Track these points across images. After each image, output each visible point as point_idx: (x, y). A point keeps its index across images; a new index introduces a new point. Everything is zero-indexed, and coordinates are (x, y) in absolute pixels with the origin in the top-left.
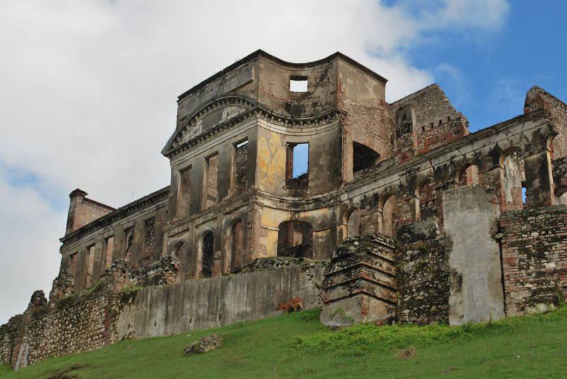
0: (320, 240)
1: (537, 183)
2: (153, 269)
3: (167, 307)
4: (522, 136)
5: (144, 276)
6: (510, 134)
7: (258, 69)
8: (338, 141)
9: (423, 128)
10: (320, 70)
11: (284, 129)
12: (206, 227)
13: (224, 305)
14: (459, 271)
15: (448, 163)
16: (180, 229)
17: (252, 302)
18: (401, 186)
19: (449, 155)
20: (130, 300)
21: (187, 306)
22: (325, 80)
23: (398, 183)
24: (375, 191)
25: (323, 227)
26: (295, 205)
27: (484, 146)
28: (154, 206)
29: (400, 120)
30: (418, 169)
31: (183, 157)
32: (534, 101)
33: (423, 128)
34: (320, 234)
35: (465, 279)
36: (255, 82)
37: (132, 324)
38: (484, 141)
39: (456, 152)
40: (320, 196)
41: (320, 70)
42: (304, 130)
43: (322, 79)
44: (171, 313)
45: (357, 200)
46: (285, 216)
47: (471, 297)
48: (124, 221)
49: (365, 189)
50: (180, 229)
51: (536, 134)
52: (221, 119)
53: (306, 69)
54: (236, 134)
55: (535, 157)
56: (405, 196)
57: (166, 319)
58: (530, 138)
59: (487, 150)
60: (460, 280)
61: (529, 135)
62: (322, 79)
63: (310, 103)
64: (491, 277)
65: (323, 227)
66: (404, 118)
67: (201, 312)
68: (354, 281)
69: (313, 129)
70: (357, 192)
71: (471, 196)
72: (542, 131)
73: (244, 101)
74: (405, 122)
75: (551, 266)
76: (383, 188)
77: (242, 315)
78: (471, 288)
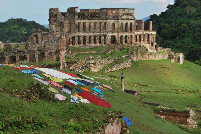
16: (122, 33)
50: (122, 33)
59: (151, 33)
61: (154, 33)
70: (136, 33)
77: (161, 58)
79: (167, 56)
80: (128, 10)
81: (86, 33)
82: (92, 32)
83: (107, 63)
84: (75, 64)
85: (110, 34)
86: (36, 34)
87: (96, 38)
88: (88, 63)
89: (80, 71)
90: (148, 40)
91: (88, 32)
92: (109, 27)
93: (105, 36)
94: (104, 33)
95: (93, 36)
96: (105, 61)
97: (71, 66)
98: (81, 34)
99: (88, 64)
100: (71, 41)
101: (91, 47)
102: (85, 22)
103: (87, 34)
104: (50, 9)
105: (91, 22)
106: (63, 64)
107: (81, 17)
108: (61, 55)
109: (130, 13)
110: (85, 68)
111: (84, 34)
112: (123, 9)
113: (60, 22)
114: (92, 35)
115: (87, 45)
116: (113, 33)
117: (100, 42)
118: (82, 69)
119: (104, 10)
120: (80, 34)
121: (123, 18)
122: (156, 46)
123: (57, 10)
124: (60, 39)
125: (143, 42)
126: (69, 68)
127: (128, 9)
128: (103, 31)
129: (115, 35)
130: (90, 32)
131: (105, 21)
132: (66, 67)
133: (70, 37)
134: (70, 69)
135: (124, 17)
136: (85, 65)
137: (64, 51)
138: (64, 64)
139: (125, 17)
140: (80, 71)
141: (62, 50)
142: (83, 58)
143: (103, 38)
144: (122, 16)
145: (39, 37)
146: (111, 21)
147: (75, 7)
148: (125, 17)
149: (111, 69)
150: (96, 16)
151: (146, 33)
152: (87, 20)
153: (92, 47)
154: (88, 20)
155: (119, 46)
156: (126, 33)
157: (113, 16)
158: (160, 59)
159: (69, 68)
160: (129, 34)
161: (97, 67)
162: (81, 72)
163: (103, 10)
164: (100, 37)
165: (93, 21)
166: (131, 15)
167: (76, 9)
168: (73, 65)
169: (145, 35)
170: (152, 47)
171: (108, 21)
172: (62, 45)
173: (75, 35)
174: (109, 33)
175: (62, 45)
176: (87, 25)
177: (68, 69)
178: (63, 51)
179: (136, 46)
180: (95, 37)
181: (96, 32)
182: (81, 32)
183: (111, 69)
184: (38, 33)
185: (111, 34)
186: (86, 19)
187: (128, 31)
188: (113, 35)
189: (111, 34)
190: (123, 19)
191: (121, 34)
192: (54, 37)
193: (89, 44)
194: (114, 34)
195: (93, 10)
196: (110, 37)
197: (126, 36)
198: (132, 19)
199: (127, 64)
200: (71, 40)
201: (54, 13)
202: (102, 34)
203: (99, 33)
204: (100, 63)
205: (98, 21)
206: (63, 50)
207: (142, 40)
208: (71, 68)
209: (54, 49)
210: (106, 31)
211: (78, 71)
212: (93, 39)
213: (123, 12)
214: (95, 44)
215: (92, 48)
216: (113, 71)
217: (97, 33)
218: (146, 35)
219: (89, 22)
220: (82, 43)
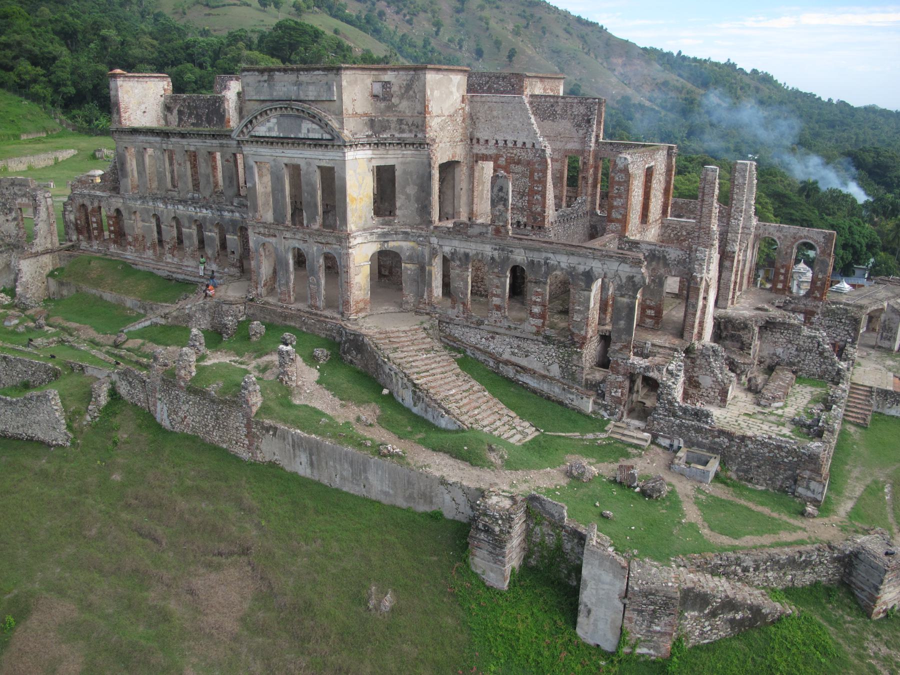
0: (409, 272)
1: (622, 323)
2: (229, 212)
4: (616, 274)
6: (605, 266)
7: (340, 87)
9: (506, 141)
10: (405, 77)
11: (370, 152)
13: (366, 478)
14: (590, 606)
15: (543, 262)
18: (492, 258)
19: (544, 255)
20: (271, 433)
22: (411, 93)
23: (490, 254)
24: (467, 251)
25: (411, 259)
26: (384, 235)
27: (579, 264)
30: (511, 252)
32: (621, 171)
33: (506, 141)
34: (409, 266)
35: (593, 612)
36: (337, 103)
37: (277, 453)
38: (580, 260)
39: (551, 255)
40: (409, 230)
41: (405, 77)
42: (390, 152)
43: (407, 91)
46: (375, 248)
47: (595, 625)
48: (184, 142)
49: (456, 243)
51: (631, 278)
52: (300, 132)
53: (389, 73)
54: (321, 157)
56: (496, 270)
58: (624, 280)
59: (581, 269)
60: (589, 612)
62: (407, 91)
63: (395, 119)
64: (613, 622)
65: (411, 259)
66: (501, 189)
67: (345, 473)
68: (497, 555)
69: (399, 152)
70: (447, 242)
71: (608, 563)
72: (636, 279)
74: (501, 194)
75: (658, 628)
76: (474, 252)
78: (596, 620)
98: (139, 202)
121: (261, 130)
135: (268, 125)
151: (537, 257)
217: (204, 211)
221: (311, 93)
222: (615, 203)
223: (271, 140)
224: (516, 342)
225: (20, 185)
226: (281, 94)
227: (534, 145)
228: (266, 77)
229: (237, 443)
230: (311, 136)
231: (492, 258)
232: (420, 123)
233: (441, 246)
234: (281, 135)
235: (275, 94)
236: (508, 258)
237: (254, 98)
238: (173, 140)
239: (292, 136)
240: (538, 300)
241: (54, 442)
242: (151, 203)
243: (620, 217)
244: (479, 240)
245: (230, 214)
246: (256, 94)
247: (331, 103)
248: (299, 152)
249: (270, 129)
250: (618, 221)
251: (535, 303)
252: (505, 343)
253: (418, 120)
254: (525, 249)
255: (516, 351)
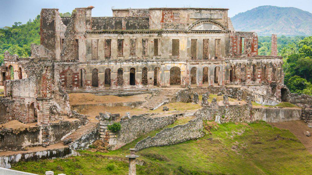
3: (267, 114)
5: (146, 63)
8: (228, 41)
12: (206, 65)
13: (279, 116)
15: (260, 62)
17: (285, 116)
19: (261, 60)
20: (257, 111)
21: (271, 114)
23: (247, 62)
24: (240, 62)
28: (148, 35)
29: (248, 43)
30: (252, 60)
31: (194, 35)
32: (256, 37)
37: (258, 117)
39: (262, 60)
44: (268, 116)
45: (235, 63)
49: (237, 61)
51: (280, 62)
52: (212, 28)
54: (217, 36)
55: (279, 69)
56: (248, 67)
57: (267, 117)
58: (279, 63)
59: (269, 62)
61: (279, 62)
67: (274, 116)
73: (219, 25)
76: (242, 62)
77: (283, 118)
79: (301, 114)
80: (209, 12)
81: (110, 62)
82: (126, 61)
83: (146, 129)
84: (74, 130)
85: (170, 65)
86: (9, 64)
87: (136, 73)
88: (101, 127)
89: (83, 145)
90: (264, 78)
91: (116, 62)
92: (167, 49)
93: (156, 70)
94: (155, 62)
95: (127, 70)
96: (141, 124)
97: (64, 134)
98: (99, 64)
99: (102, 130)
100: (77, 79)
101: (122, 94)
102: (108, 38)
103: (113, 64)
104: (44, 11)
105: (123, 38)
106: (45, 129)
107: (104, 28)
108: (41, 110)
109: (212, 18)
110: (96, 138)
111: (106, 64)
112: (197, 9)
113: (61, 39)
114: (125, 67)
115: (115, 88)
116: (175, 62)
117: (145, 82)
118: (88, 139)
119: (156, 11)
120: (98, 66)
121: (197, 28)
122: (283, 91)
123: (54, 12)
124: (39, 78)
125: (251, 82)
126: (58, 137)
127: (210, 10)
128: (152, 58)
129: (179, 66)
130: (121, 61)
131: (155, 36)
132: (53, 135)
133: (74, 70)
134: (62, 139)
135: (200, 27)
136: (95, 132)
137: (47, 103)
138: (46, 129)
139: (201, 27)
140: (83, 145)
141: (42, 100)
142: (95, 116)
143: (150, 74)
144: (195, 25)
145: (15, 70)
146: (169, 35)
147: (87, 7)
148: (201, 27)
149: (153, 141)
150: (138, 25)
151: (259, 61)
152: (112, 35)
153: (125, 93)
154: (116, 35)
155: (186, 92)
156: (204, 62)
157: (175, 25)
158: (282, 121)
159: (58, 137)
160: (212, 63)
161: (122, 136)
162: (86, 146)
163: (154, 13)
164: (145, 70)
165: (127, 38)
166: (216, 23)
167: (88, 12)
168: (68, 132)
169: (254, 66)
170: (274, 93)
171: (164, 35)
172: (42, 90)
173: (84, 67)
174: (167, 62)
175: (42, 90)
176: (114, 45)
177: (56, 140)
178: (44, 102)
179: (229, 91)
180: (133, 69)
181: (134, 60)
182: (99, 61)
183: (153, 141)
184: (14, 63)
185: (170, 65)
186: (109, 33)
187: (210, 58)
188: (176, 65)
189: (170, 65)
190: (197, 32)
191: (193, 64)
192: (34, 72)
193: (119, 87)
194: (176, 64)
195: (139, 11)
196: (169, 72)
197: (205, 70)
198: (218, 32)
199: (193, 131)
200: (76, 78)
201: (48, 19)
202: (150, 63)
203: (142, 61)
204: (129, 129)
205: (139, 37)
206: (46, 100)
207: (249, 78)
208: (64, 137)
209: (29, 97)
210: (159, 57)
211: (78, 144)
212: (127, 76)
213: (195, 17)
214: (132, 86)
215: (123, 95)
216: (156, 146)
217: (138, 63)
218: (258, 67)
219: (119, 38)
220: (101, 85)
221: (215, 17)
222: (255, 47)
223: (217, 31)
224: (254, 87)
225: (43, 61)
226: (205, 17)
227: (233, 32)
228: (198, 11)
229: (246, 119)
230: (215, 30)
231: (247, 64)
232: (227, 26)
233: (233, 62)
234: (205, 30)
235: (202, 17)
236: (251, 63)
237: (194, 18)
238: (125, 35)
239: (209, 30)
240: (259, 73)
241: (198, 137)
242: (106, 64)
243: (256, 50)
244: (244, 58)
245: (152, 63)
246: (195, 17)
247: (221, 20)
248: (217, 35)
249: (200, 28)
250: (256, 52)
251: (259, 74)
252: (252, 88)
253: (226, 25)
254: (256, 59)
255: (255, 90)
